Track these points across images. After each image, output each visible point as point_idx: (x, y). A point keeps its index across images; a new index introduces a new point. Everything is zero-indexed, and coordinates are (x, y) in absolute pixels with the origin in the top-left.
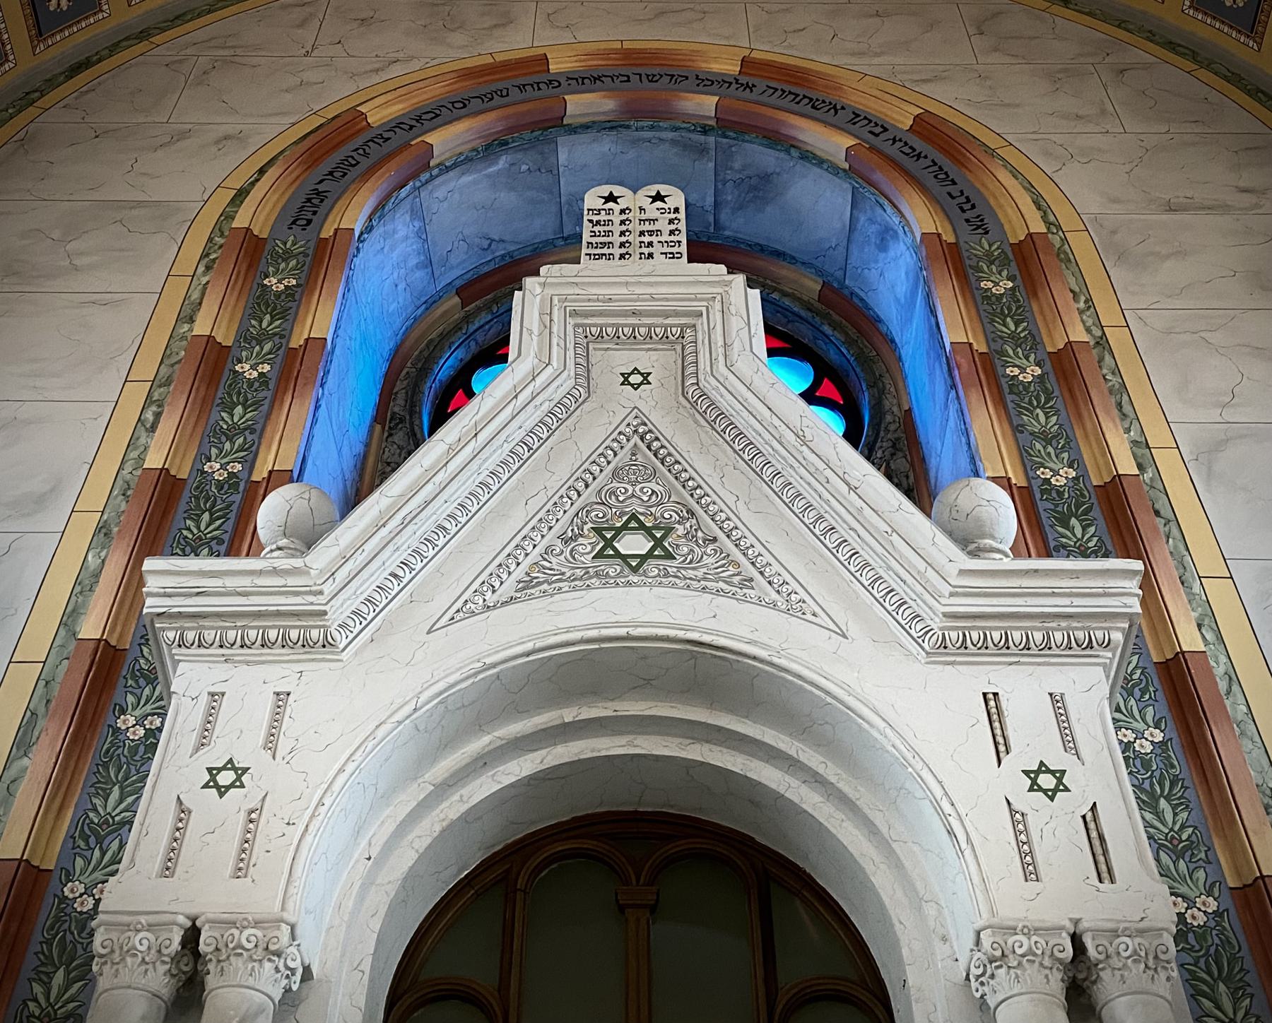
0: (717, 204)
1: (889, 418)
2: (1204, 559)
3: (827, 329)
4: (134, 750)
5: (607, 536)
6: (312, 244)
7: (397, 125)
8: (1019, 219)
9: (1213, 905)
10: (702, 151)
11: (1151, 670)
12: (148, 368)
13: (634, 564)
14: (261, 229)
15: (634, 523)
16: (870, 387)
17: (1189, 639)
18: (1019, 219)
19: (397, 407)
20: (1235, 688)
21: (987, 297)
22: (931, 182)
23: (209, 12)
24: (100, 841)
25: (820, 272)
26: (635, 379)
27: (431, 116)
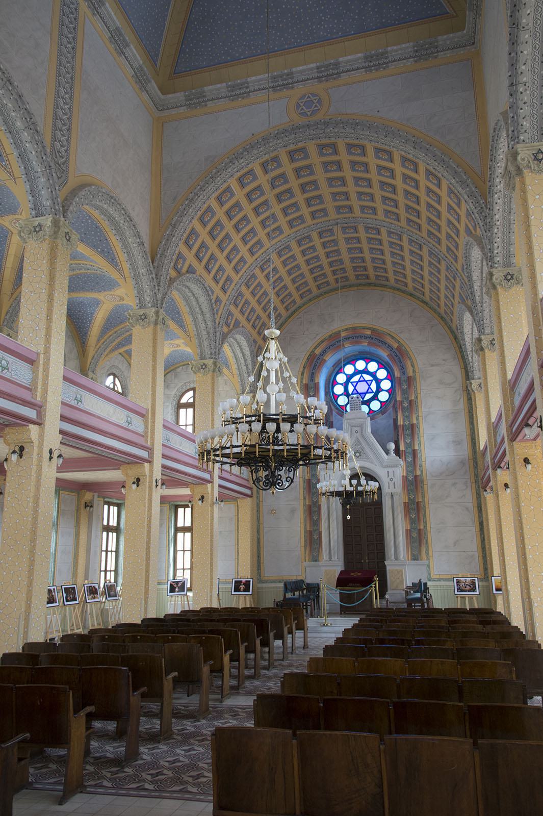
2: (421, 435)
7: (321, 355)
15: (357, 452)
17: (416, 447)
19: (327, 390)
21: (403, 390)
26: (357, 432)
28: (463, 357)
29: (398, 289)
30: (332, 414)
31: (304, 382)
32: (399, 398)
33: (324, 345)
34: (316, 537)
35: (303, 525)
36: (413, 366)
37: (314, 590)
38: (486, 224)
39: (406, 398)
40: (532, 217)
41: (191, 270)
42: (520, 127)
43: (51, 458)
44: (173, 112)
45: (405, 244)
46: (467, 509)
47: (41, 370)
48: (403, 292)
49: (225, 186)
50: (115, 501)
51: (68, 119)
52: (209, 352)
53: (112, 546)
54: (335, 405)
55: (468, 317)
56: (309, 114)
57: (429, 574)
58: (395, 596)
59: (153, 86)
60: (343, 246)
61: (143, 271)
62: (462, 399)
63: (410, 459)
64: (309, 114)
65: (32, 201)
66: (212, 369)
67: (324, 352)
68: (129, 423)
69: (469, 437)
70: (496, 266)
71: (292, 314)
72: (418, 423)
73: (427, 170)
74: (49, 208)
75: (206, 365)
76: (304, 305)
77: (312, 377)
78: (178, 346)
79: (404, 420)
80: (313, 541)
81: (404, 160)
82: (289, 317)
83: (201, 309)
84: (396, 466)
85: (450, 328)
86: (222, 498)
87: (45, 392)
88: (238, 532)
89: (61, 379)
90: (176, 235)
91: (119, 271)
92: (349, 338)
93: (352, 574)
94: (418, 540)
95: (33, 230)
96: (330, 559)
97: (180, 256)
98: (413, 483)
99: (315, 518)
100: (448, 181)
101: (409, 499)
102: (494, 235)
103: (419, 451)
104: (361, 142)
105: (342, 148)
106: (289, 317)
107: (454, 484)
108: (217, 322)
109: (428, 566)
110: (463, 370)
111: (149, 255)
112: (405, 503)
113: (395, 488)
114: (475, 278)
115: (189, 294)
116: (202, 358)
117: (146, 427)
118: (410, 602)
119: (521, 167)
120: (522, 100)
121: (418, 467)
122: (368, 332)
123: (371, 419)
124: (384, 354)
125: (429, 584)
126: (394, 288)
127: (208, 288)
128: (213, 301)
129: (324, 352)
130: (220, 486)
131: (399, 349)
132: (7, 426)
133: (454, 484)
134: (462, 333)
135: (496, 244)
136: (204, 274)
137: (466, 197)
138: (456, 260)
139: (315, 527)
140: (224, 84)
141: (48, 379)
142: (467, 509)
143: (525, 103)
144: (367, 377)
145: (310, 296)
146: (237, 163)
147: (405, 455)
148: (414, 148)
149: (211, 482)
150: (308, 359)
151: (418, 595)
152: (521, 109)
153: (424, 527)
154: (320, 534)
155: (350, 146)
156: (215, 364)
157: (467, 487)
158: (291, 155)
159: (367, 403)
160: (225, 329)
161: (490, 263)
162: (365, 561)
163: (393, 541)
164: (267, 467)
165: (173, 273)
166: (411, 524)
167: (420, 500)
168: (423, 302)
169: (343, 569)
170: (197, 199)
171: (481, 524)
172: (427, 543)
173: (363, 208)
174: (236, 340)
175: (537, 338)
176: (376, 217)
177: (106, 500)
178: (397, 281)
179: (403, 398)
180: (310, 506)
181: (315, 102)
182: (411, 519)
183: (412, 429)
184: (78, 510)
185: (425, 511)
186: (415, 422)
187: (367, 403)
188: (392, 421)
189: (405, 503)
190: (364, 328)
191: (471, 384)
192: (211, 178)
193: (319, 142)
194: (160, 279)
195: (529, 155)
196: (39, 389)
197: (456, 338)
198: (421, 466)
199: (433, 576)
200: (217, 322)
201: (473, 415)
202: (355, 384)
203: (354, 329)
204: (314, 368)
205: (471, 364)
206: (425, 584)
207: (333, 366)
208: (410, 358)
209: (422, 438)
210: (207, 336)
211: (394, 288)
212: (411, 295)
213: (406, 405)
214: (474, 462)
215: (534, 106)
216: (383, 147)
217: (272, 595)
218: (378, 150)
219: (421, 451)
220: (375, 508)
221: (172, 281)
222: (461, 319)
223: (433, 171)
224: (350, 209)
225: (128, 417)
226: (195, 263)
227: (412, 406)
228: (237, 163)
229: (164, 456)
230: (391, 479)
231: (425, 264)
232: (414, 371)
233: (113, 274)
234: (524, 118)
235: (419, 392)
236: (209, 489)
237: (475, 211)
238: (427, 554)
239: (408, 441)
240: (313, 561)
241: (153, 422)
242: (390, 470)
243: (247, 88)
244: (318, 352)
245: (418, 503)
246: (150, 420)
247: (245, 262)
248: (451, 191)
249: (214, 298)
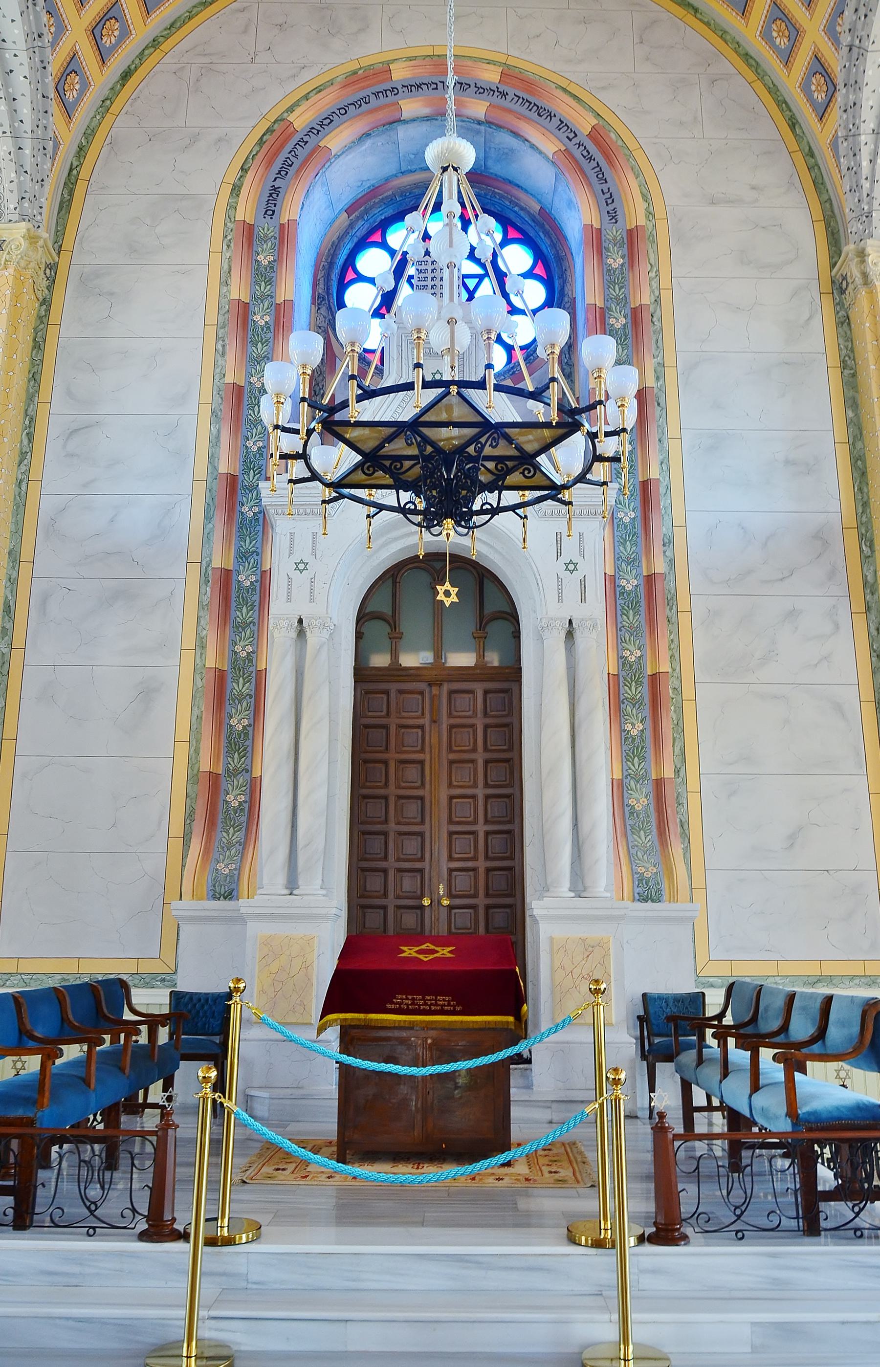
0: (485, 158)
1: (566, 299)
2: (672, 430)
3: (541, 234)
4: (251, 522)
6: (277, 230)
9: (636, 583)
10: (478, 132)
11: (638, 487)
12: (213, 318)
16: (559, 278)
17: (654, 473)
18: (635, 214)
19: (321, 290)
20: (668, 491)
21: (610, 271)
22: (594, 180)
23: (190, 18)
24: (247, 560)
25: (540, 202)
27: (326, 123)
31: (240, 217)
34: (234, 798)
39: (623, 301)
46: (839, 708)
62: (817, 321)
67: (326, 123)
69: (844, 452)
72: (663, 390)
77: (272, 200)
92: (419, 86)
93: (409, 952)
94: (654, 814)
96: (292, 885)
99: (238, 722)
101: (623, 661)
103: (662, 490)
107: (792, 614)
110: (821, 227)
113: (583, 599)
131: (596, 135)
133: (792, 614)
139: (236, 761)
142: (839, 708)
150: (261, 142)
153: (677, 772)
154: (254, 788)
157: (837, 627)
162: (436, 902)
166: (627, 758)
167: (665, 667)
172: (685, 836)
179: (607, 298)
180: (220, 677)
182: (624, 737)
185: (680, 710)
198: (668, 542)
204: (282, 173)
205: (866, 185)
207: (349, 210)
209: (673, 446)
214: (861, 537)
219: (668, 487)
220: (486, 692)
232: (650, 214)
240: (215, 898)
244: (301, 120)
245: (655, 679)
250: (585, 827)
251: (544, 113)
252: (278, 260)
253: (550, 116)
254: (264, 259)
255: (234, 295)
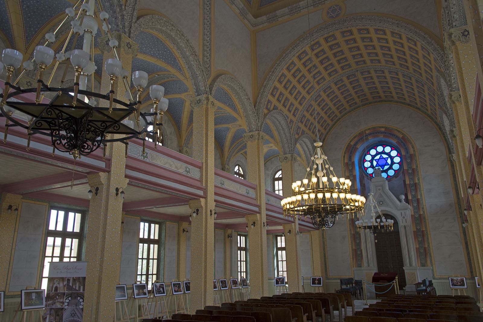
2: (422, 189)
5: (379, 202)
8: (412, 152)
13: (381, 204)
14: (347, 162)
15: (381, 201)
17: (419, 197)
18: (412, 152)
19: (360, 165)
26: (379, 189)
28: (446, 140)
29: (400, 102)
30: (364, 179)
31: (345, 162)
32: (405, 168)
33: (356, 139)
34: (359, 253)
35: (350, 246)
36: (413, 147)
37: (359, 283)
38: (446, 66)
40: (464, 69)
41: (275, 108)
42: (452, 18)
43: (211, 214)
44: (261, 27)
45: (401, 77)
47: (204, 171)
48: (404, 103)
49: (291, 61)
50: (243, 234)
51: (210, 44)
52: (288, 150)
53: (243, 258)
54: (365, 174)
55: (444, 116)
56: (334, 16)
57: (434, 275)
58: (410, 288)
59: (250, 16)
60: (362, 82)
61: (250, 113)
63: (415, 205)
64: (334, 16)
65: (195, 89)
66: (290, 159)
67: (356, 144)
68: (248, 193)
70: (454, 90)
71: (336, 123)
72: (419, 182)
73: (407, 38)
74: (203, 91)
75: (287, 158)
76: (342, 117)
77: (350, 158)
78: (271, 147)
79: (410, 181)
80: (357, 255)
81: (393, 33)
82: (334, 125)
83: (282, 127)
84: (406, 209)
85: (436, 123)
86: (301, 231)
87: (207, 181)
88: (312, 250)
89: (214, 174)
90: (266, 91)
91: (238, 114)
93: (382, 275)
94: (424, 254)
95: (196, 102)
96: (369, 266)
97: (269, 101)
98: (419, 219)
99: (358, 241)
100: (420, 42)
101: (417, 229)
102: (451, 72)
104: (366, 27)
105: (355, 31)
106: (334, 125)
108: (292, 133)
109: (433, 270)
111: (252, 104)
112: (414, 231)
113: (406, 222)
114: (445, 94)
115: (275, 120)
116: (285, 153)
117: (257, 195)
118: (419, 292)
119: (455, 41)
120: (452, 3)
121: (421, 209)
122: (383, 130)
123: (388, 181)
124: (394, 142)
125: (433, 281)
126: (397, 102)
127: (285, 116)
128: (289, 122)
129: (356, 144)
130: (299, 224)
131: (403, 138)
132: (190, 199)
134: (443, 125)
135: (452, 77)
136: (283, 109)
137: (432, 51)
138: (433, 84)
140: (287, 8)
141: (207, 175)
143: (454, 5)
144: (385, 156)
145: (346, 112)
146: (296, 49)
147: (412, 202)
148: (398, 27)
149: (294, 222)
150: (347, 148)
151: (424, 288)
152: (452, 8)
153: (428, 246)
154: (361, 251)
155: (359, 30)
156: (292, 156)
158: (326, 40)
159: (386, 171)
160: (297, 136)
161: (450, 89)
163: (407, 256)
164: (320, 216)
165: (266, 111)
167: (424, 229)
168: (417, 108)
169: (377, 272)
170: (276, 71)
171: (466, 243)
172: (431, 256)
173: (372, 61)
174: (303, 141)
175: (472, 137)
176: (380, 64)
177: (239, 233)
178: (399, 98)
181: (338, 9)
183: (416, 186)
184: (225, 239)
185: (428, 236)
186: (417, 181)
187: (386, 171)
188: (402, 182)
189: (414, 231)
190: (380, 127)
191: (453, 156)
192: (283, 59)
193: (341, 30)
194: (259, 116)
195: (459, 33)
196: (204, 181)
197: (440, 128)
198: (423, 208)
199: (436, 277)
200: (292, 133)
201: (455, 175)
202: (377, 161)
203: (374, 128)
205: (452, 144)
206: (430, 282)
207: (363, 151)
208: (411, 143)
209: (422, 192)
210: (286, 141)
211: (397, 102)
212: (409, 105)
213: (410, 171)
215: (460, 5)
216: (379, 28)
217: (335, 287)
218: (376, 30)
219: (422, 199)
221: (265, 115)
222: (442, 118)
223: (411, 38)
224: (364, 62)
225: (247, 190)
226: (277, 104)
227: (414, 172)
228: (296, 49)
229: (267, 210)
230: (404, 217)
231: (415, 87)
232: (414, 151)
233: (235, 115)
234: (454, 13)
235: (418, 163)
236: (293, 226)
237: (439, 59)
238: (431, 262)
239: (414, 193)
240: (358, 267)
241: (260, 192)
242: (403, 212)
243: (299, 8)
244: (352, 143)
245: (423, 231)
246: (258, 191)
247: (305, 99)
248: (423, 48)
249: (289, 120)
250: (410, 256)
251: (393, 135)
252: (352, 168)
253: (394, 135)
254: (350, 168)
255: (347, 175)
